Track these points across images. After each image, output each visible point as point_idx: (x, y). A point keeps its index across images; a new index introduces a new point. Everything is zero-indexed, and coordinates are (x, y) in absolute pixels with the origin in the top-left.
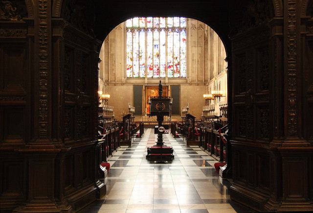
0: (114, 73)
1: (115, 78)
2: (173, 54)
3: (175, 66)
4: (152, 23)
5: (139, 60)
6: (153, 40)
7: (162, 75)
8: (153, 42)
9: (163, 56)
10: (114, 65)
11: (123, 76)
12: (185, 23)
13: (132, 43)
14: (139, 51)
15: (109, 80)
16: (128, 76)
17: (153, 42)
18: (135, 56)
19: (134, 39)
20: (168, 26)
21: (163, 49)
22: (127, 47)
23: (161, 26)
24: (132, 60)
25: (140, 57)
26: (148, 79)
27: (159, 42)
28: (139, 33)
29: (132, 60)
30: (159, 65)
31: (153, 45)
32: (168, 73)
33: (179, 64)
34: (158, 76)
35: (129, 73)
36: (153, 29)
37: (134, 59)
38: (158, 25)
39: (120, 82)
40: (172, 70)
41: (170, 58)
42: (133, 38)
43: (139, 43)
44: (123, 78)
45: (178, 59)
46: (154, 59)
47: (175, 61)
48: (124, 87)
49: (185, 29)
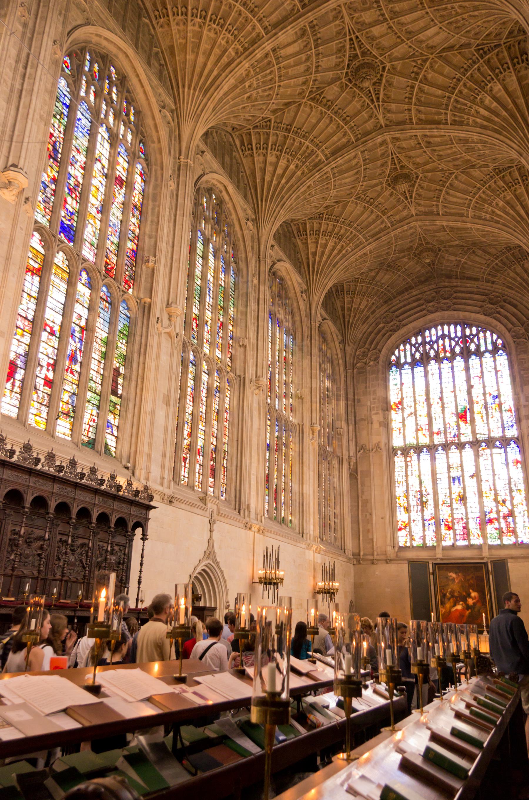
0: (370, 537)
1: (373, 549)
2: (496, 495)
3: (502, 521)
4: (442, 434)
5: (422, 511)
6: (449, 467)
7: (476, 541)
8: (449, 472)
9: (472, 499)
10: (369, 521)
11: (389, 542)
12: (515, 427)
13: (407, 476)
14: (421, 492)
15: (362, 553)
16: (401, 545)
17: (449, 472)
18: (413, 501)
19: (409, 469)
20: (478, 436)
21: (471, 484)
22: (397, 485)
23: (463, 439)
24: (407, 510)
25: (423, 504)
26: (444, 548)
27: (462, 470)
28: (419, 456)
29: (407, 510)
30: (467, 519)
31: (449, 477)
32: (488, 536)
33: (511, 514)
34: (466, 543)
35: (402, 539)
36: (446, 447)
37: (412, 508)
38: (458, 436)
39: (383, 557)
40: (496, 529)
41: (489, 504)
42: (407, 466)
43: (420, 476)
44: (389, 548)
45: (508, 503)
46: (455, 506)
47: (500, 508)
48: (392, 568)
49: (517, 441)
